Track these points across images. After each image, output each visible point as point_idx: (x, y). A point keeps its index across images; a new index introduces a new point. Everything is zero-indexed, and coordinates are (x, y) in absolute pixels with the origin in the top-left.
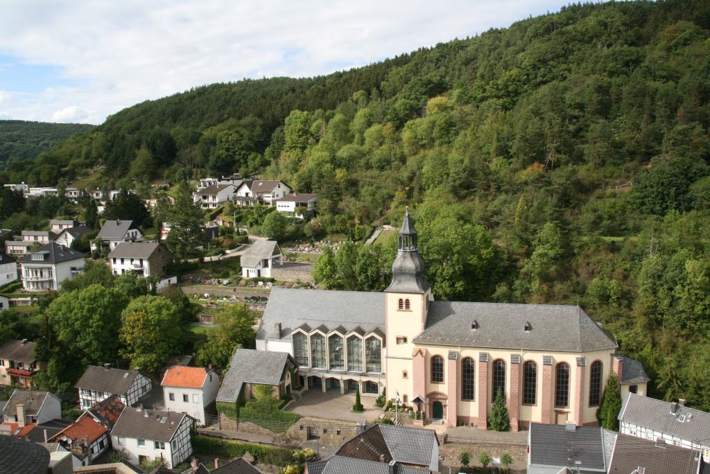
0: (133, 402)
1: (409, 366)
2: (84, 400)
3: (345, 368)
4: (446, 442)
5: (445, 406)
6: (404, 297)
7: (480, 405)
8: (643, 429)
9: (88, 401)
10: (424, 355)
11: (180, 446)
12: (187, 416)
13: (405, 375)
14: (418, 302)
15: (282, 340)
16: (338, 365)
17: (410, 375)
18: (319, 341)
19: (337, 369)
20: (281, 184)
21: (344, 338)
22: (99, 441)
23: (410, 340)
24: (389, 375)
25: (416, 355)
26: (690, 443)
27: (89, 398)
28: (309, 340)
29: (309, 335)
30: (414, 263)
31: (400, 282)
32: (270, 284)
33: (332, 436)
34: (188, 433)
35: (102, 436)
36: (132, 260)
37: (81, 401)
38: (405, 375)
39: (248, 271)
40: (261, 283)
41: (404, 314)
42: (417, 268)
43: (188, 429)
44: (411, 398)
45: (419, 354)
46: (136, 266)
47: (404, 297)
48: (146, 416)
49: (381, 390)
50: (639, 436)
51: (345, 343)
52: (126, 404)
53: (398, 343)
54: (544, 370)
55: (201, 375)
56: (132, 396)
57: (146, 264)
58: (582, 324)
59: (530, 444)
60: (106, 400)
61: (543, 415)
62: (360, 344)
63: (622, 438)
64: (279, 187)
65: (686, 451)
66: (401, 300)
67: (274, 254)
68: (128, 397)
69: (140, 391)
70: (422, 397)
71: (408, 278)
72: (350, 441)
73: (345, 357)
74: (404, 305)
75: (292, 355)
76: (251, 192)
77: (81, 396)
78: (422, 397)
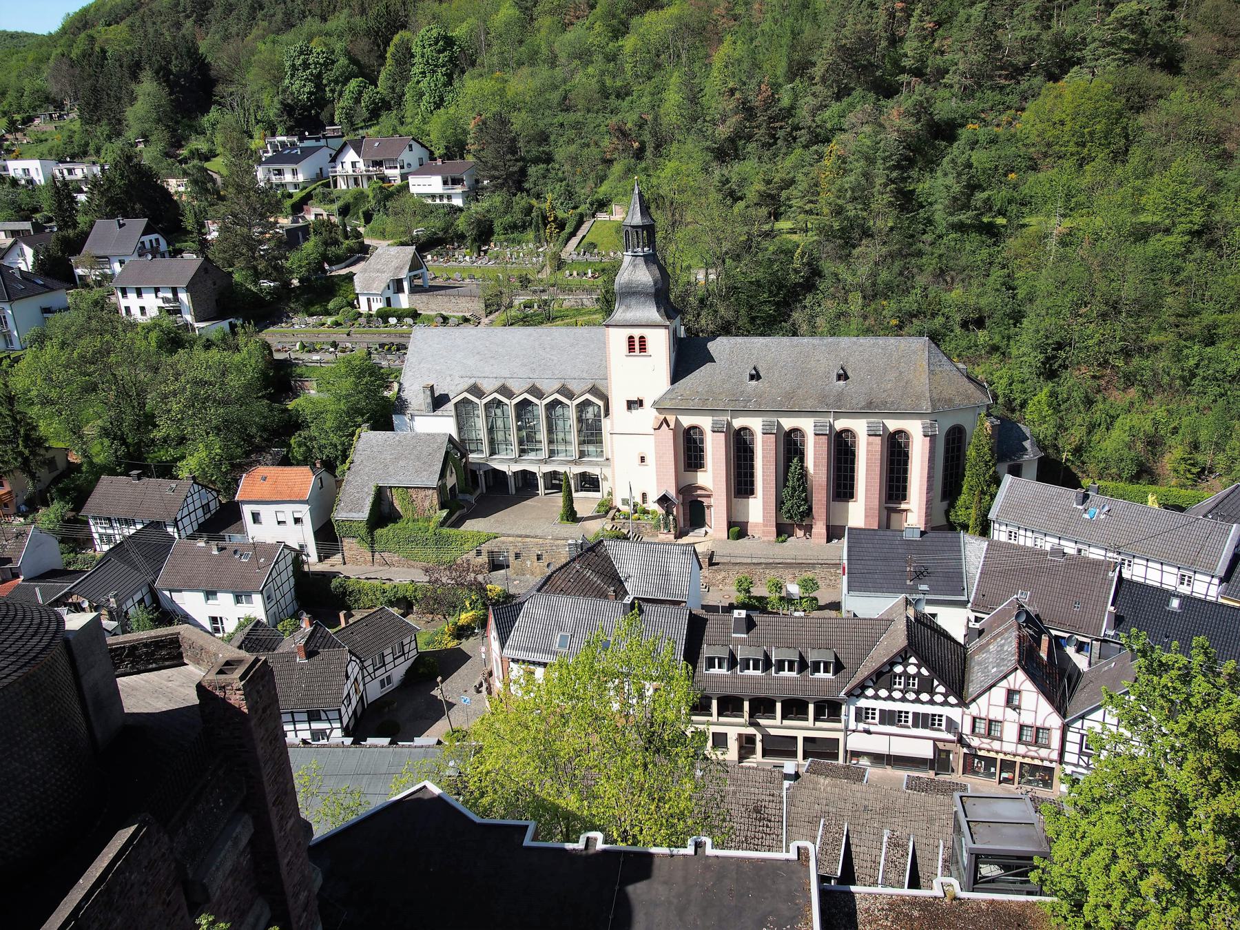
0: (189, 531)
1: (648, 446)
2: (101, 535)
3: (544, 454)
4: (711, 564)
5: (709, 507)
6: (637, 333)
7: (764, 502)
8: (1029, 534)
9: (109, 536)
10: (672, 426)
11: (279, 597)
12: (286, 546)
13: (643, 459)
14: (659, 341)
15: (439, 412)
16: (532, 450)
17: (650, 459)
18: (499, 412)
19: (532, 456)
20: (412, 142)
22: (137, 597)
23: (648, 403)
24: (617, 461)
25: (659, 427)
26: (1103, 552)
27: (110, 531)
28: (481, 412)
29: (481, 403)
30: (651, 274)
31: (628, 307)
32: (409, 321)
33: (529, 563)
34: (291, 574)
35: (141, 589)
36: (157, 290)
37: (96, 536)
38: (643, 459)
39: (369, 300)
40: (393, 321)
41: (638, 361)
42: (656, 283)
43: (291, 568)
44: (653, 496)
46: (166, 300)
47: (637, 333)
48: (215, 552)
49: (605, 486)
50: (1021, 543)
51: (541, 412)
52: (176, 535)
53: (629, 408)
54: (868, 444)
55: (303, 479)
56: (186, 521)
57: (184, 297)
58: (932, 368)
59: (846, 562)
60: (138, 532)
61: (866, 516)
62: (566, 413)
63: (994, 546)
64: (411, 150)
65: (1096, 564)
66: (631, 338)
67: (410, 270)
68: (180, 523)
69: (200, 512)
70: (672, 493)
71: (642, 299)
72: (560, 569)
73: (542, 435)
74: (637, 346)
75: (455, 436)
76: (361, 160)
77: (93, 529)
78: (672, 493)
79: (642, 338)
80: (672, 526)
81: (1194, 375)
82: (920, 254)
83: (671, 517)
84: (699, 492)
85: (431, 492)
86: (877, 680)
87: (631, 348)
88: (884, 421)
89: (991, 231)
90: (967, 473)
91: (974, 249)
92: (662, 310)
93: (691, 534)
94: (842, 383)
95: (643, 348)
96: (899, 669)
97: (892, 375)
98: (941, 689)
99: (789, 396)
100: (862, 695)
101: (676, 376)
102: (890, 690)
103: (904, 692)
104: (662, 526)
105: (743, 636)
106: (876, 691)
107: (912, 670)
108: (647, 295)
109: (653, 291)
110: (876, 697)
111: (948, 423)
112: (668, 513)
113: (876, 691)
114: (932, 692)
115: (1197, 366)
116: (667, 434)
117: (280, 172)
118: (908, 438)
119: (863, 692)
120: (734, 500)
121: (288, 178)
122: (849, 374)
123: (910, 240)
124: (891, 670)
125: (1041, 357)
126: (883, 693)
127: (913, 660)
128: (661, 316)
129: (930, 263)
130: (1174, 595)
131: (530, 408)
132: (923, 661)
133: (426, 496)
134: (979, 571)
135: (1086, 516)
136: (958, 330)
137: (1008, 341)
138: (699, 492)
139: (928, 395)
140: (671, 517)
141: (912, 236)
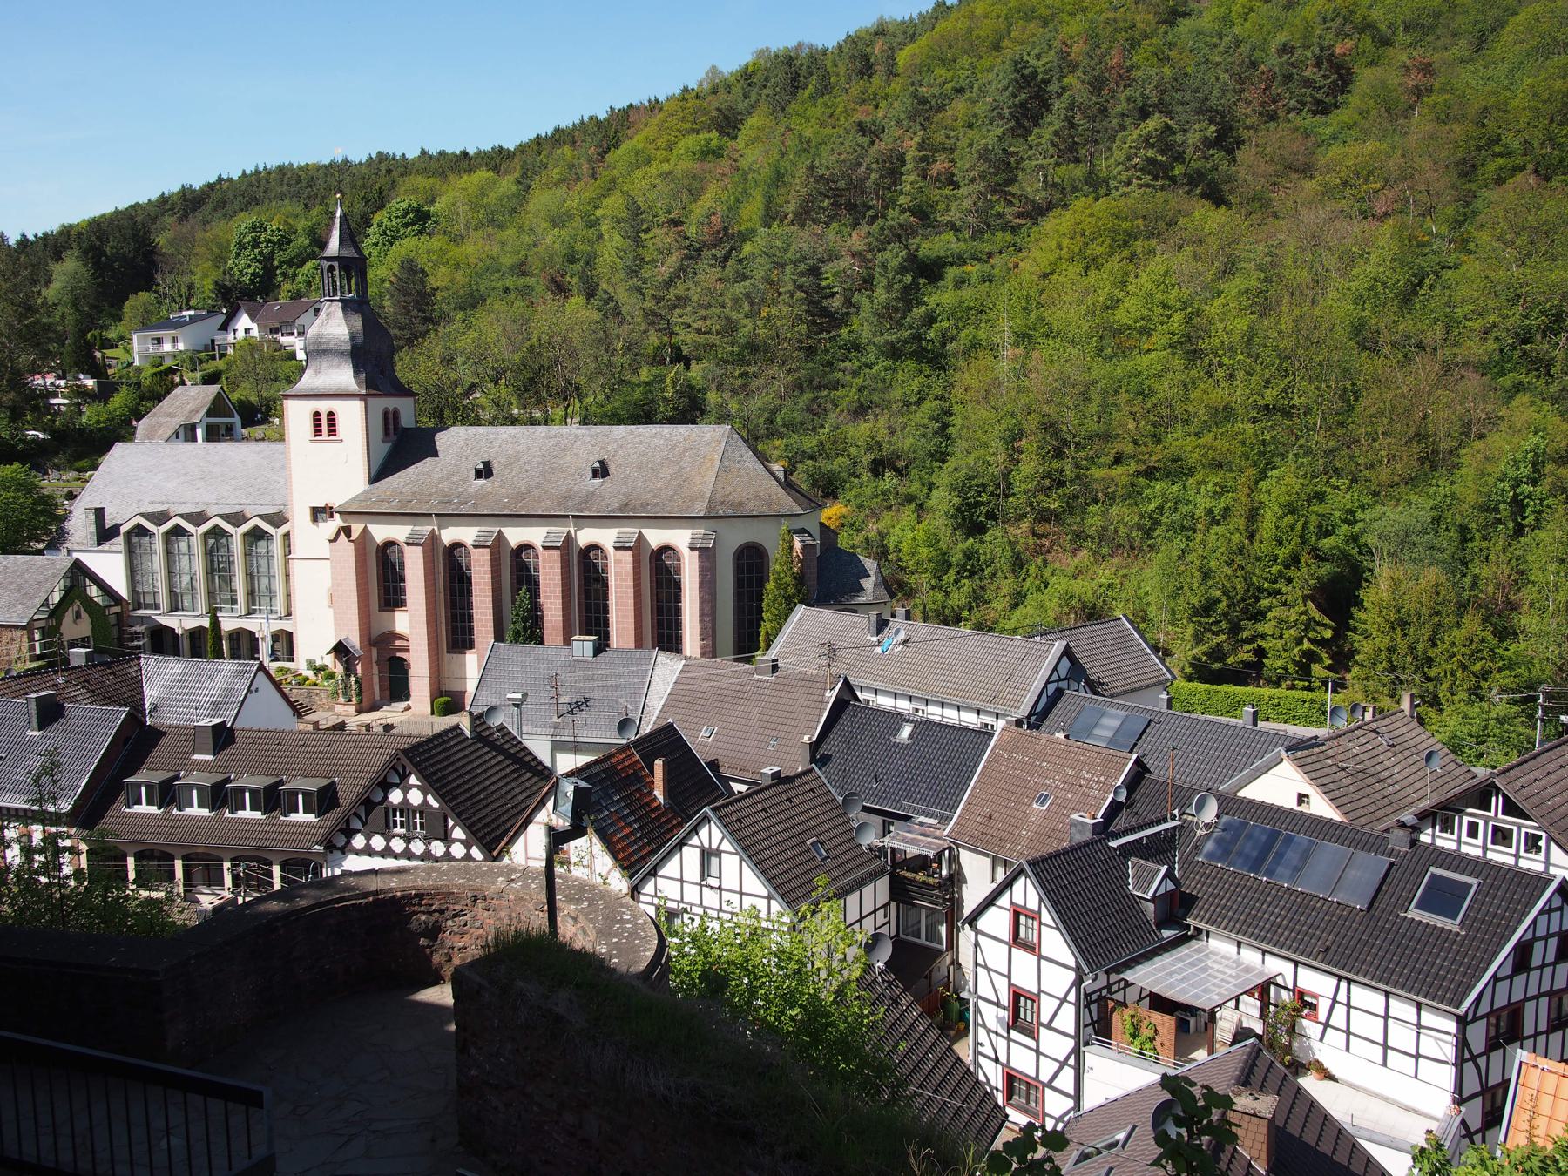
6: (324, 406)
10: (354, 536)
15: (105, 547)
21: (237, 532)
25: (335, 539)
28: (158, 544)
30: (350, 328)
31: (317, 372)
41: (326, 447)
42: (353, 337)
45: (342, 535)
47: (324, 406)
51: (237, 547)
53: (315, 519)
66: (317, 415)
67: (209, 414)
70: (354, 640)
71: (336, 361)
73: (239, 583)
74: (325, 426)
78: (354, 640)
79: (331, 414)
80: (353, 693)
81: (1156, 523)
82: (837, 385)
83: (353, 679)
84: (398, 643)
85: (19, 633)
86: (367, 816)
87: (317, 431)
88: (643, 531)
89: (935, 360)
90: (766, 615)
91: (908, 379)
92: (363, 377)
93: (385, 708)
94: (598, 481)
95: (332, 431)
96: (396, 797)
97: (666, 473)
98: (458, 833)
99: (520, 496)
100: (346, 849)
101: (378, 474)
102: (388, 839)
103: (408, 840)
104: (340, 692)
105: (210, 757)
106: (368, 838)
107: (415, 798)
108: (342, 353)
109: (349, 348)
110: (368, 851)
111: (736, 537)
112: (349, 670)
113: (368, 838)
114: (447, 839)
115: (1161, 509)
116: (346, 548)
117: (159, 341)
118: (679, 559)
119: (349, 842)
120: (447, 657)
121: (167, 347)
122: (612, 469)
123: (827, 369)
124: (386, 798)
125: (957, 501)
126: (378, 842)
127: (413, 780)
128: (358, 384)
129: (848, 397)
130: (908, 721)
131: (224, 541)
132: (431, 783)
133: (13, 639)
134: (662, 702)
135: (879, 650)
136: (866, 476)
137: (930, 489)
138: (398, 643)
139: (708, 495)
140: (353, 679)
141: (830, 364)
